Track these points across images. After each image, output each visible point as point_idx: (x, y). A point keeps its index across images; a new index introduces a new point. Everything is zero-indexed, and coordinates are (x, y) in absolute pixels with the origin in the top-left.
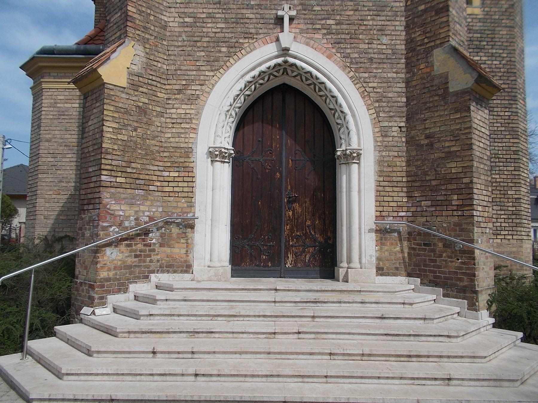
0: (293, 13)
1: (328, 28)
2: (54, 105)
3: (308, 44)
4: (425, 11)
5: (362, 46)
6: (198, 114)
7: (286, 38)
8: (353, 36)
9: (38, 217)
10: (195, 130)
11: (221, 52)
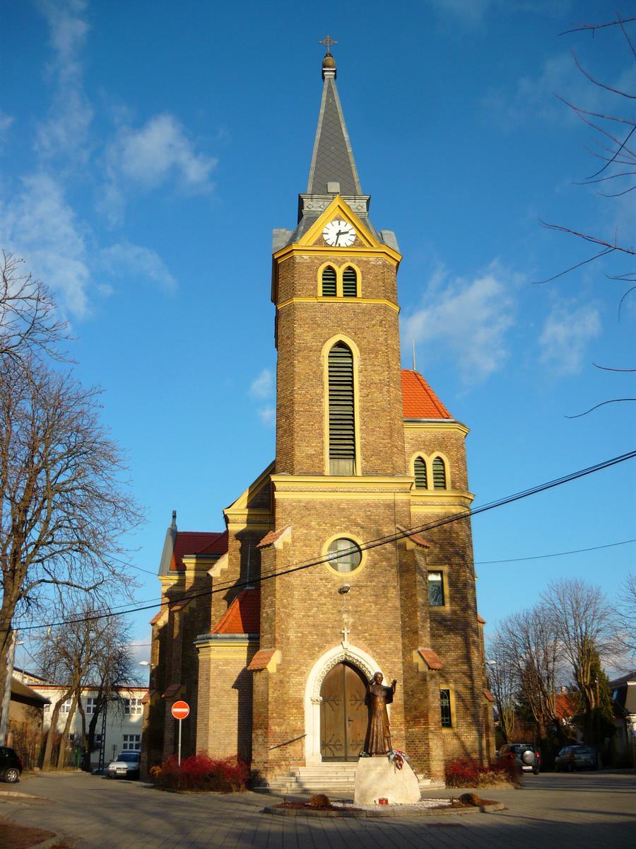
0: (349, 632)
1: (365, 637)
2: (216, 667)
3: (356, 645)
4: (409, 631)
5: (382, 646)
6: (305, 681)
7: (346, 643)
8: (377, 641)
9: (210, 732)
10: (304, 689)
11: (314, 651)
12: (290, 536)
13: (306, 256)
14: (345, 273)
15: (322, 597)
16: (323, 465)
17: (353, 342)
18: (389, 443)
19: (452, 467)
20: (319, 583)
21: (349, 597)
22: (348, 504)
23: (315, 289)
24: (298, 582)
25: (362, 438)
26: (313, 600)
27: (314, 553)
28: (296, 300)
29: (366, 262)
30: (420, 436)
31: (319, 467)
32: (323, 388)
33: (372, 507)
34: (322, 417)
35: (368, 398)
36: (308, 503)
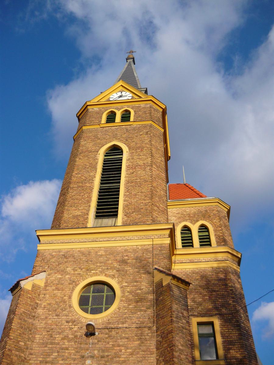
12: (44, 281)
13: (96, 108)
14: (123, 114)
15: (66, 341)
16: (87, 222)
17: (123, 144)
18: (149, 202)
19: (215, 231)
20: (65, 325)
21: (96, 341)
22: (106, 251)
23: (100, 121)
24: (43, 325)
25: (125, 201)
26: (54, 343)
27: (65, 296)
28: (84, 128)
29: (138, 107)
30: (185, 211)
31: (83, 224)
32: (96, 172)
33: (129, 252)
34: (91, 189)
35: (133, 175)
36: (67, 252)
